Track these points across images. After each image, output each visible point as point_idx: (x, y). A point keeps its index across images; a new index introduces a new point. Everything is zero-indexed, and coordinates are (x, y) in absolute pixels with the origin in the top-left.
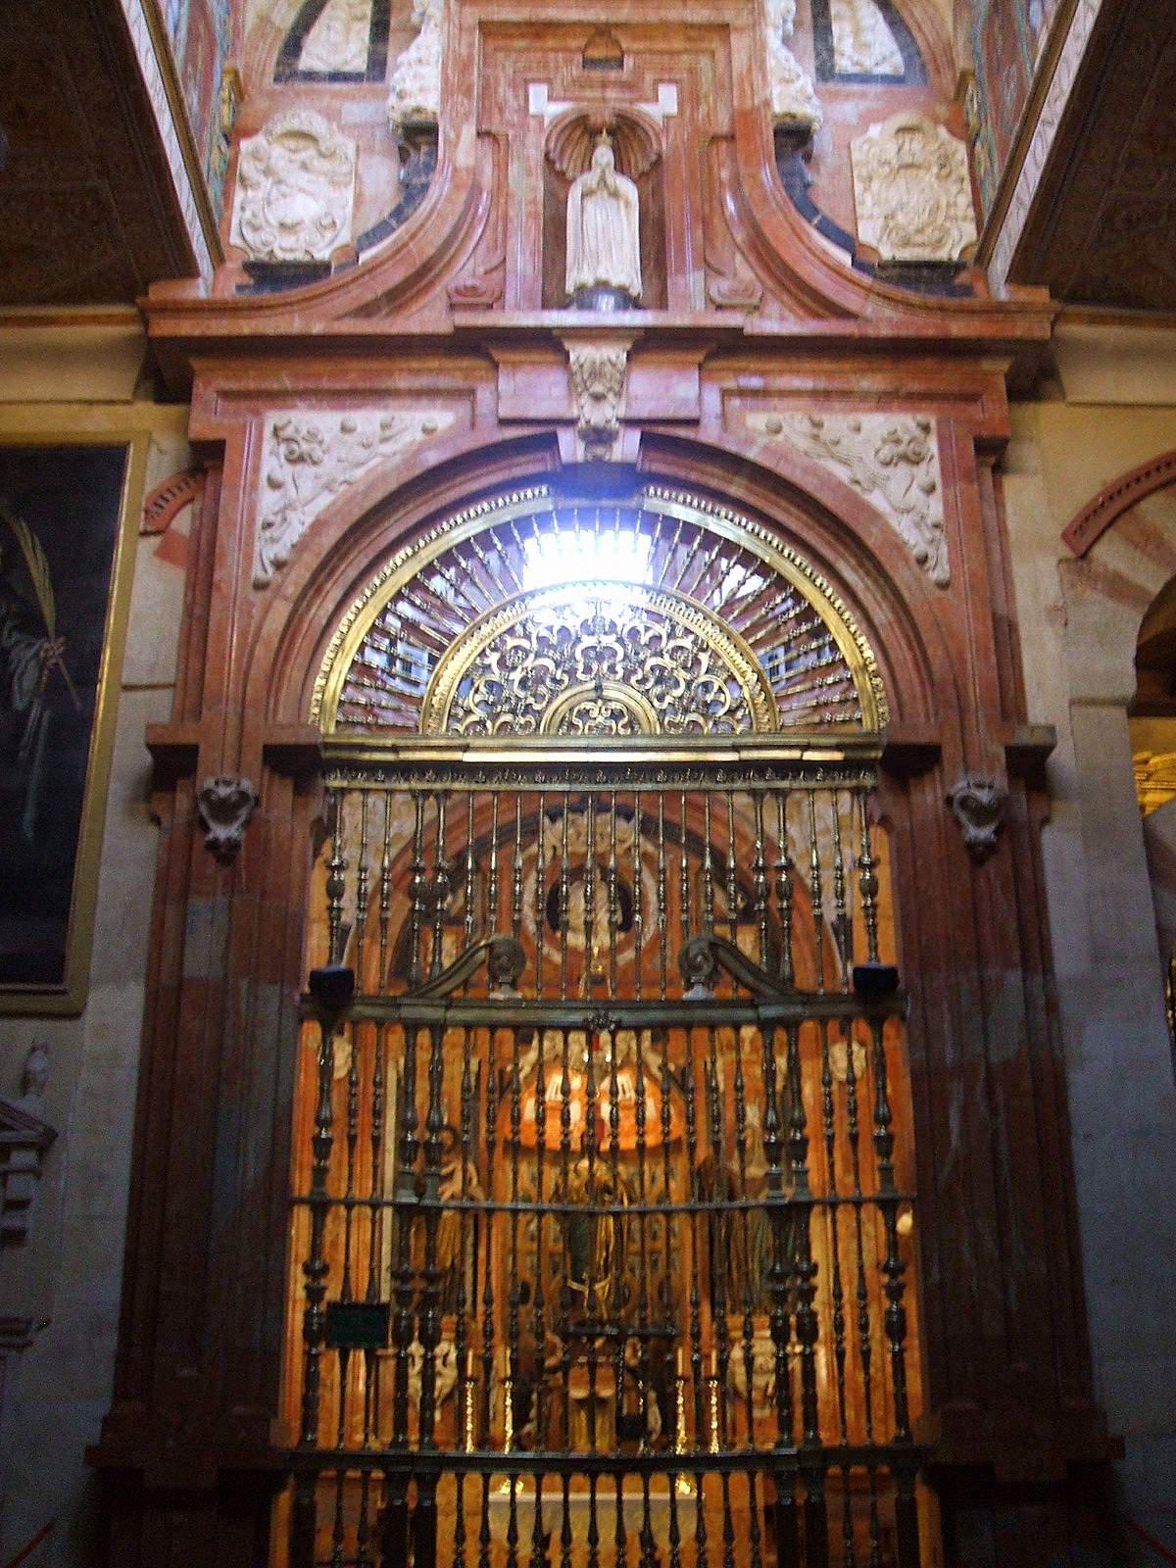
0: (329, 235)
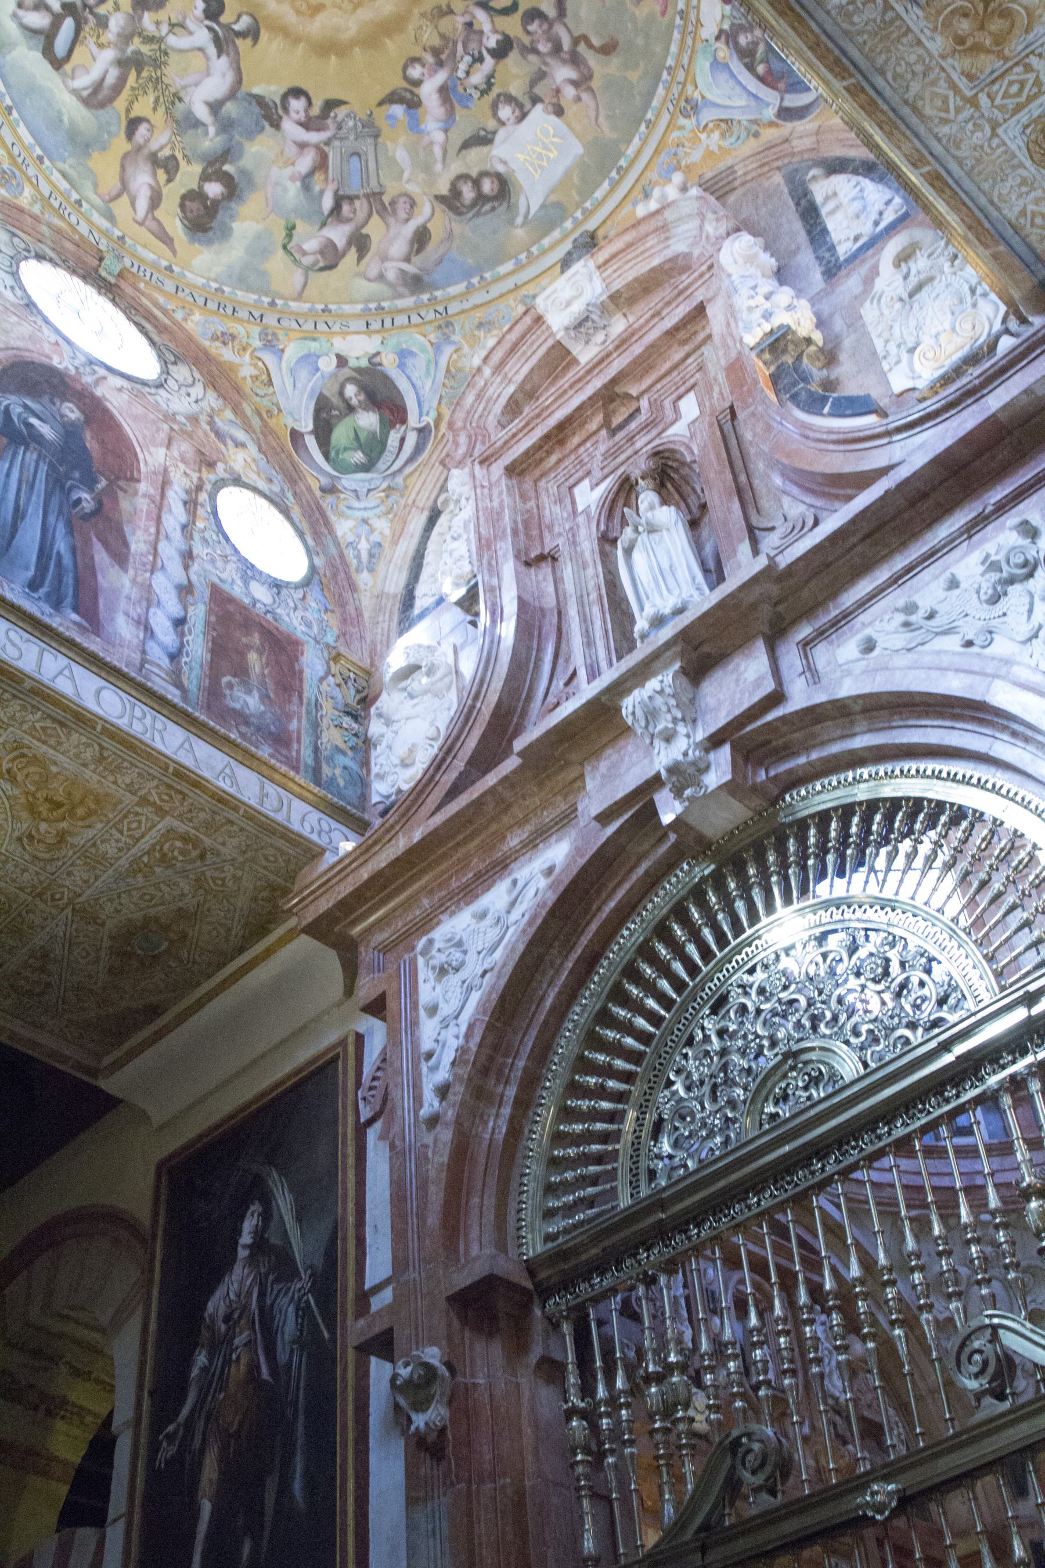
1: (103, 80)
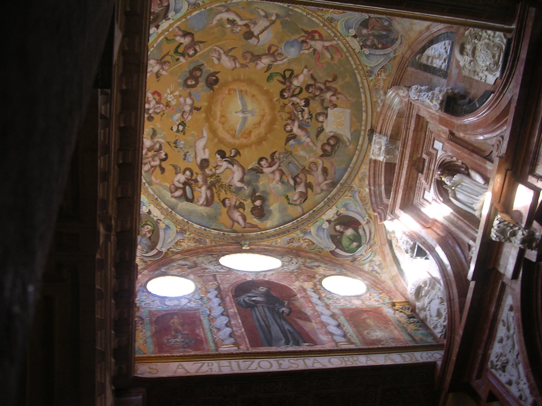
1: (207, 196)
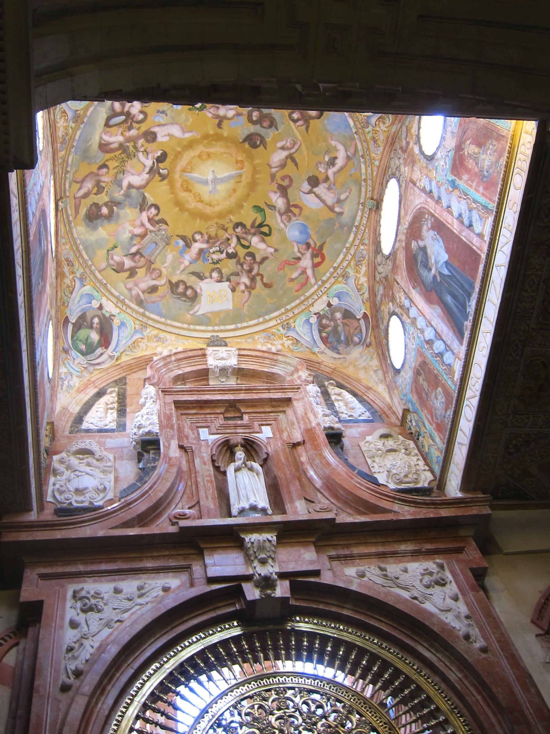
0: (102, 495)
1: (111, 144)
